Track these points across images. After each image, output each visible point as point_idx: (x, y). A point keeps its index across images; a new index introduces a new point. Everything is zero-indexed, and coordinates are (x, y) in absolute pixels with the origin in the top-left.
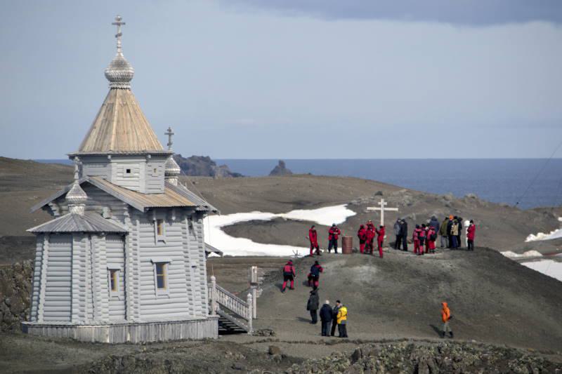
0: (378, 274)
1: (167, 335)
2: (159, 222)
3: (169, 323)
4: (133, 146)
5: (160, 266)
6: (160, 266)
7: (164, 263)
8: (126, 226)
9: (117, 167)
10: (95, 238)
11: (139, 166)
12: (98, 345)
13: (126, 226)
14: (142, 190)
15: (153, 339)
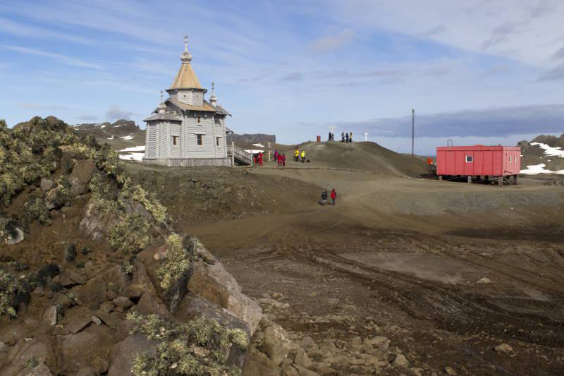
0: (324, 147)
1: (202, 163)
2: (199, 118)
3: (202, 159)
4: (188, 86)
5: (199, 136)
6: (199, 136)
7: (201, 135)
8: (181, 118)
9: (180, 94)
10: (165, 123)
11: (190, 94)
12: (165, 167)
13: (181, 118)
14: (191, 104)
15: (193, 165)
